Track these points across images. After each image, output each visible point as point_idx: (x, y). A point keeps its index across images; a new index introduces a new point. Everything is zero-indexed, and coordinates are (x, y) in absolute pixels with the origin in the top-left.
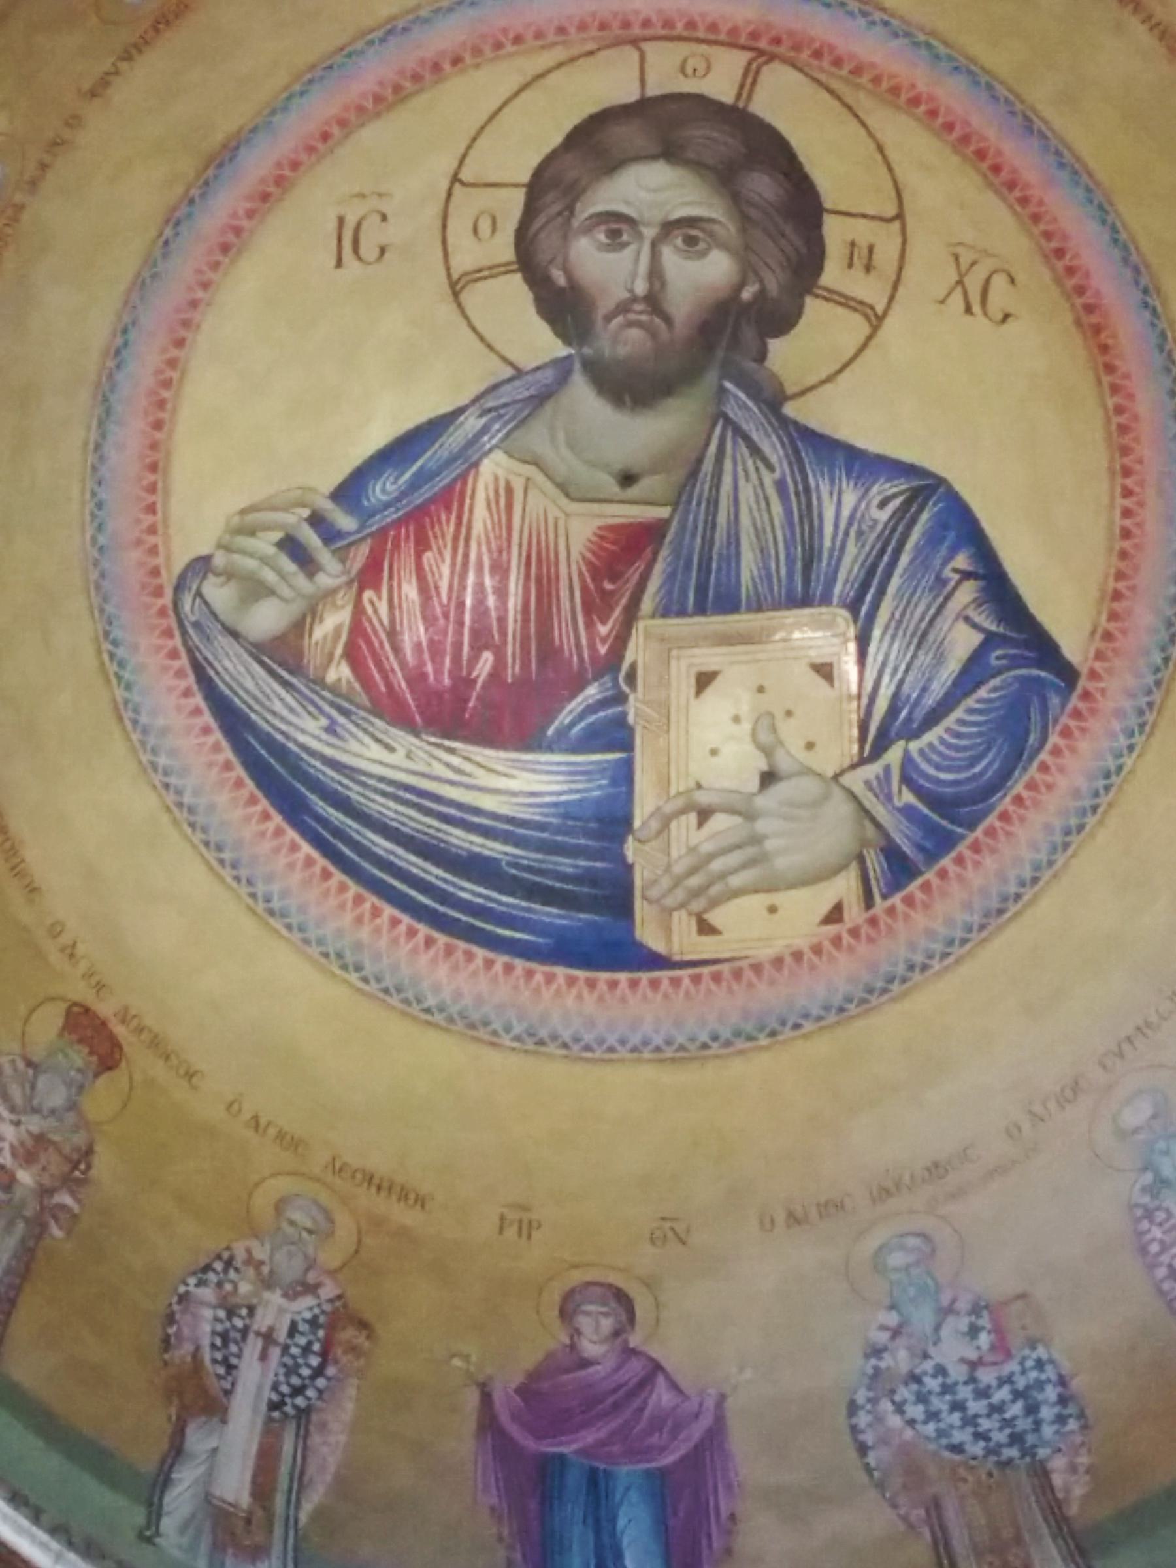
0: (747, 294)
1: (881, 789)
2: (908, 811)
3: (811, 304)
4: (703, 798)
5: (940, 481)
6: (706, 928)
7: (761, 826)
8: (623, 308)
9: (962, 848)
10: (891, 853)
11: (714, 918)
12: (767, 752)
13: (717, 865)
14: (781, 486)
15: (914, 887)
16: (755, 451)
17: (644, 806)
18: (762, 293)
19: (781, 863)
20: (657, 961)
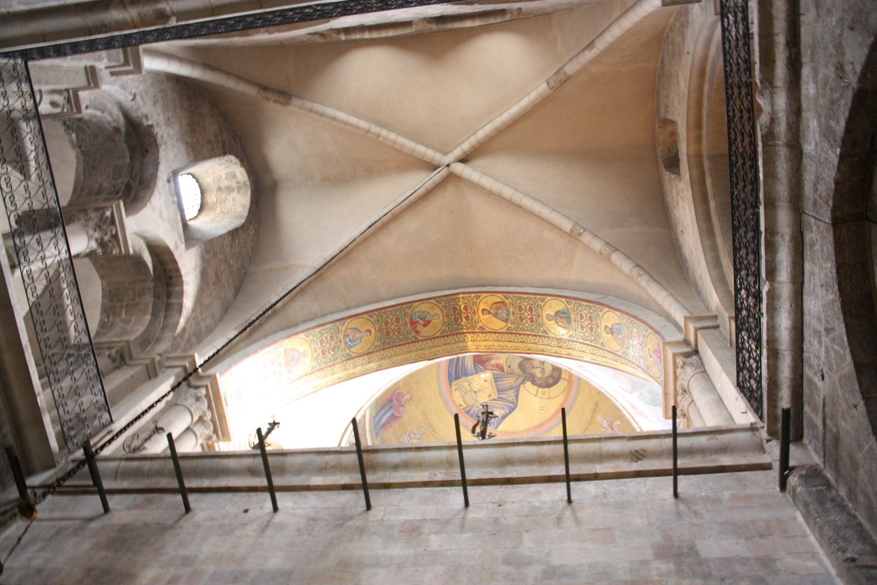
0: (536, 379)
1: (477, 407)
2: (475, 411)
3: (536, 387)
4: (471, 385)
5: (516, 406)
6: (456, 390)
7: (469, 393)
8: (531, 363)
9: (472, 419)
10: (470, 410)
11: (457, 391)
12: (479, 391)
13: (463, 389)
14: (512, 385)
15: (466, 415)
16: (516, 381)
17: (469, 378)
18: (536, 381)
19: (465, 397)
20: (450, 385)
